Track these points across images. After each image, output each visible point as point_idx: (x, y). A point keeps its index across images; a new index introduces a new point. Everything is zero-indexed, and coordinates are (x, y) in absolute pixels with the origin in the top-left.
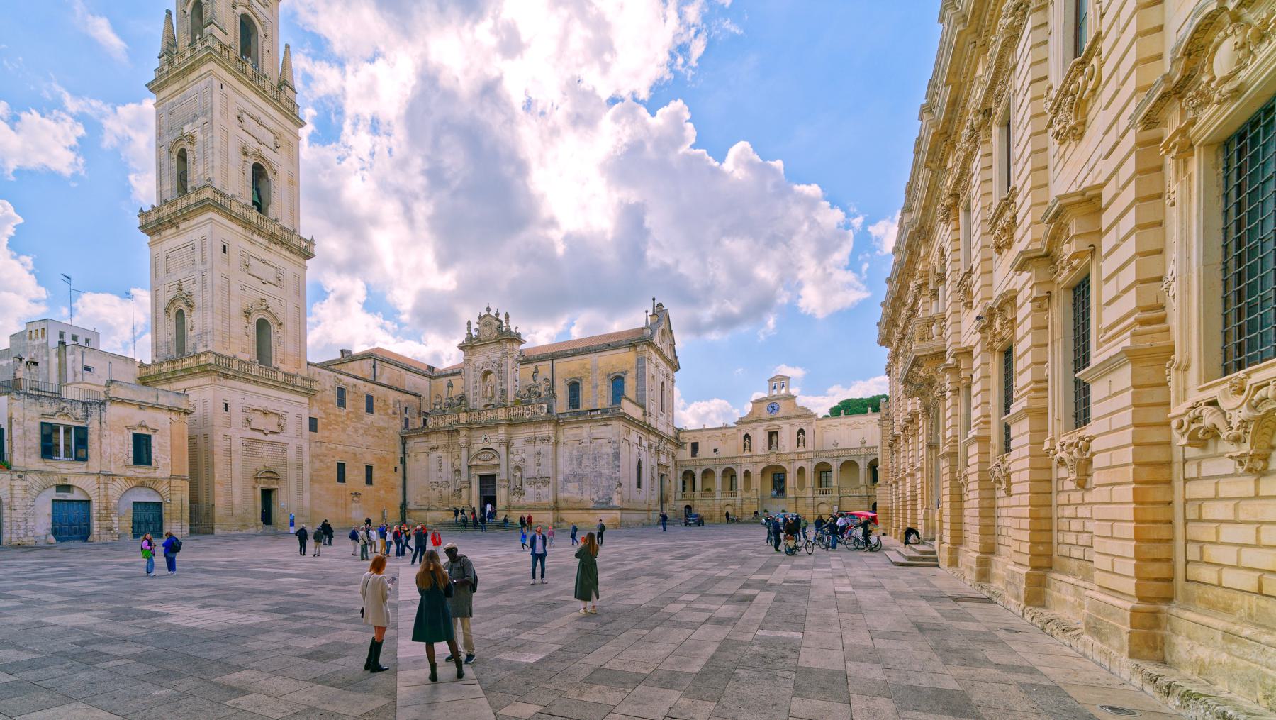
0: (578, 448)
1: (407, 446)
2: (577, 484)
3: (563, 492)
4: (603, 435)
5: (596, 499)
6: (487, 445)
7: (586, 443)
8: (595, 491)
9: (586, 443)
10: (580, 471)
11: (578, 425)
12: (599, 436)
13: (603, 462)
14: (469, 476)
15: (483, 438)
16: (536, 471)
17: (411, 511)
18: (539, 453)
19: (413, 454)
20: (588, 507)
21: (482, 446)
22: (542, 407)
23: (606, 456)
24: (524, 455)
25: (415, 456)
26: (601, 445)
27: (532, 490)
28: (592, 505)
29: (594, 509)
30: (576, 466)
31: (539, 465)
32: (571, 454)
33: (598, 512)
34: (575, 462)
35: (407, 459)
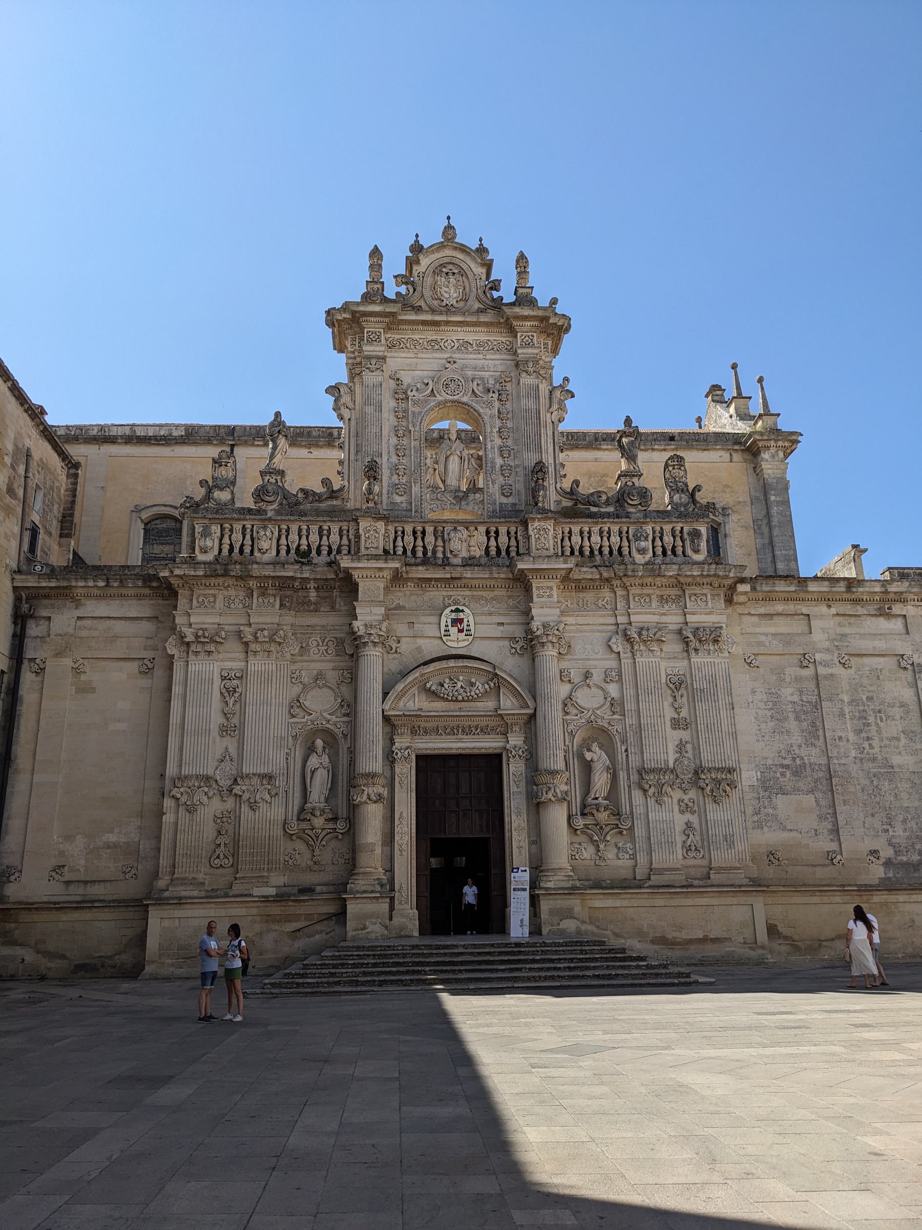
0: (798, 679)
1: (33, 629)
2: (809, 800)
3: (759, 825)
4: (880, 645)
5: (887, 853)
6: (457, 642)
7: (826, 665)
8: (878, 825)
9: (826, 665)
10: (813, 755)
11: (791, 607)
12: (867, 645)
13: (893, 728)
14: (390, 758)
15: (447, 616)
16: (671, 748)
17: (30, 907)
18: (677, 685)
19: (67, 662)
20: (863, 880)
21: (431, 648)
22: (696, 534)
23: (897, 712)
24: (613, 690)
25: (77, 671)
26: (876, 674)
27: (656, 815)
28: (877, 872)
29: (888, 886)
30: (796, 738)
31: (676, 724)
32: (775, 702)
33: (902, 897)
34: (793, 725)
35: (28, 678)
